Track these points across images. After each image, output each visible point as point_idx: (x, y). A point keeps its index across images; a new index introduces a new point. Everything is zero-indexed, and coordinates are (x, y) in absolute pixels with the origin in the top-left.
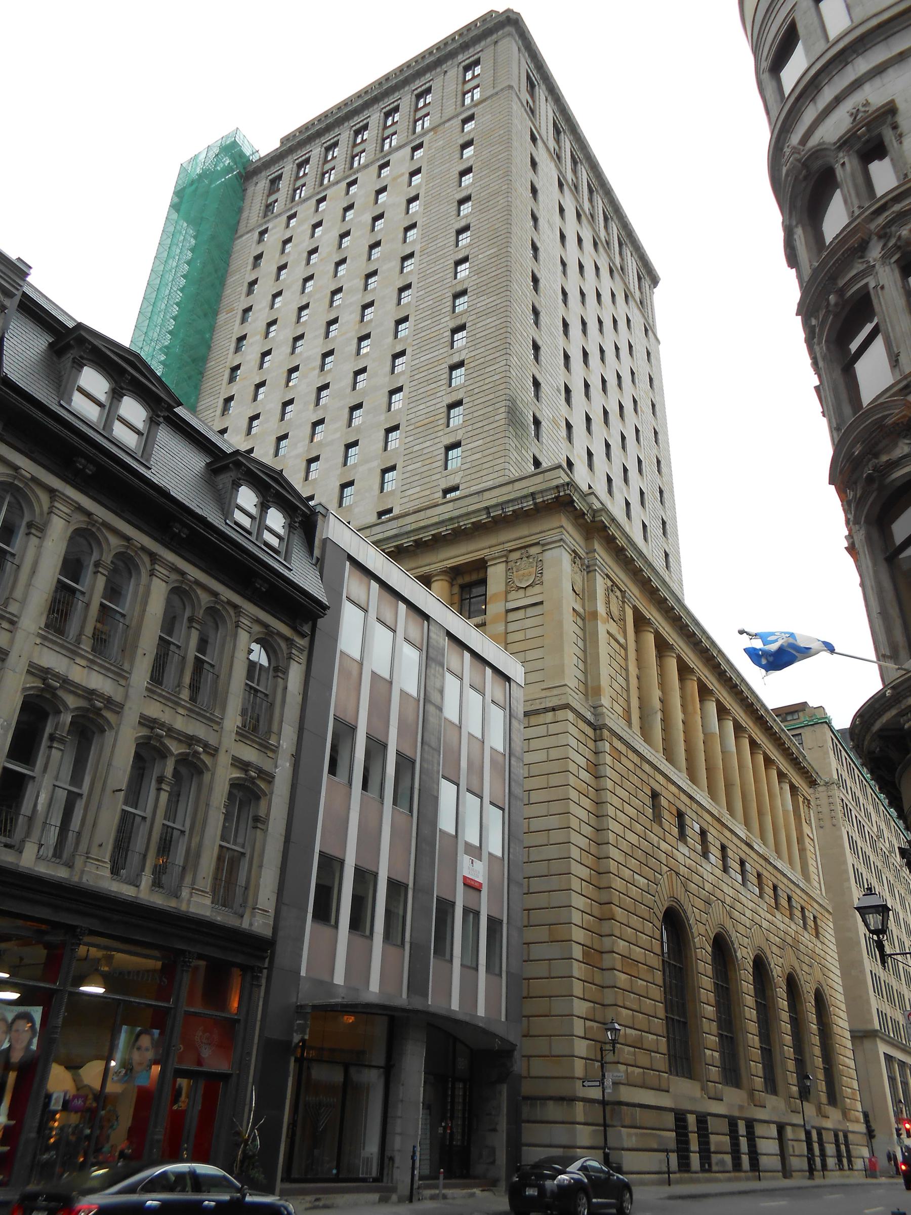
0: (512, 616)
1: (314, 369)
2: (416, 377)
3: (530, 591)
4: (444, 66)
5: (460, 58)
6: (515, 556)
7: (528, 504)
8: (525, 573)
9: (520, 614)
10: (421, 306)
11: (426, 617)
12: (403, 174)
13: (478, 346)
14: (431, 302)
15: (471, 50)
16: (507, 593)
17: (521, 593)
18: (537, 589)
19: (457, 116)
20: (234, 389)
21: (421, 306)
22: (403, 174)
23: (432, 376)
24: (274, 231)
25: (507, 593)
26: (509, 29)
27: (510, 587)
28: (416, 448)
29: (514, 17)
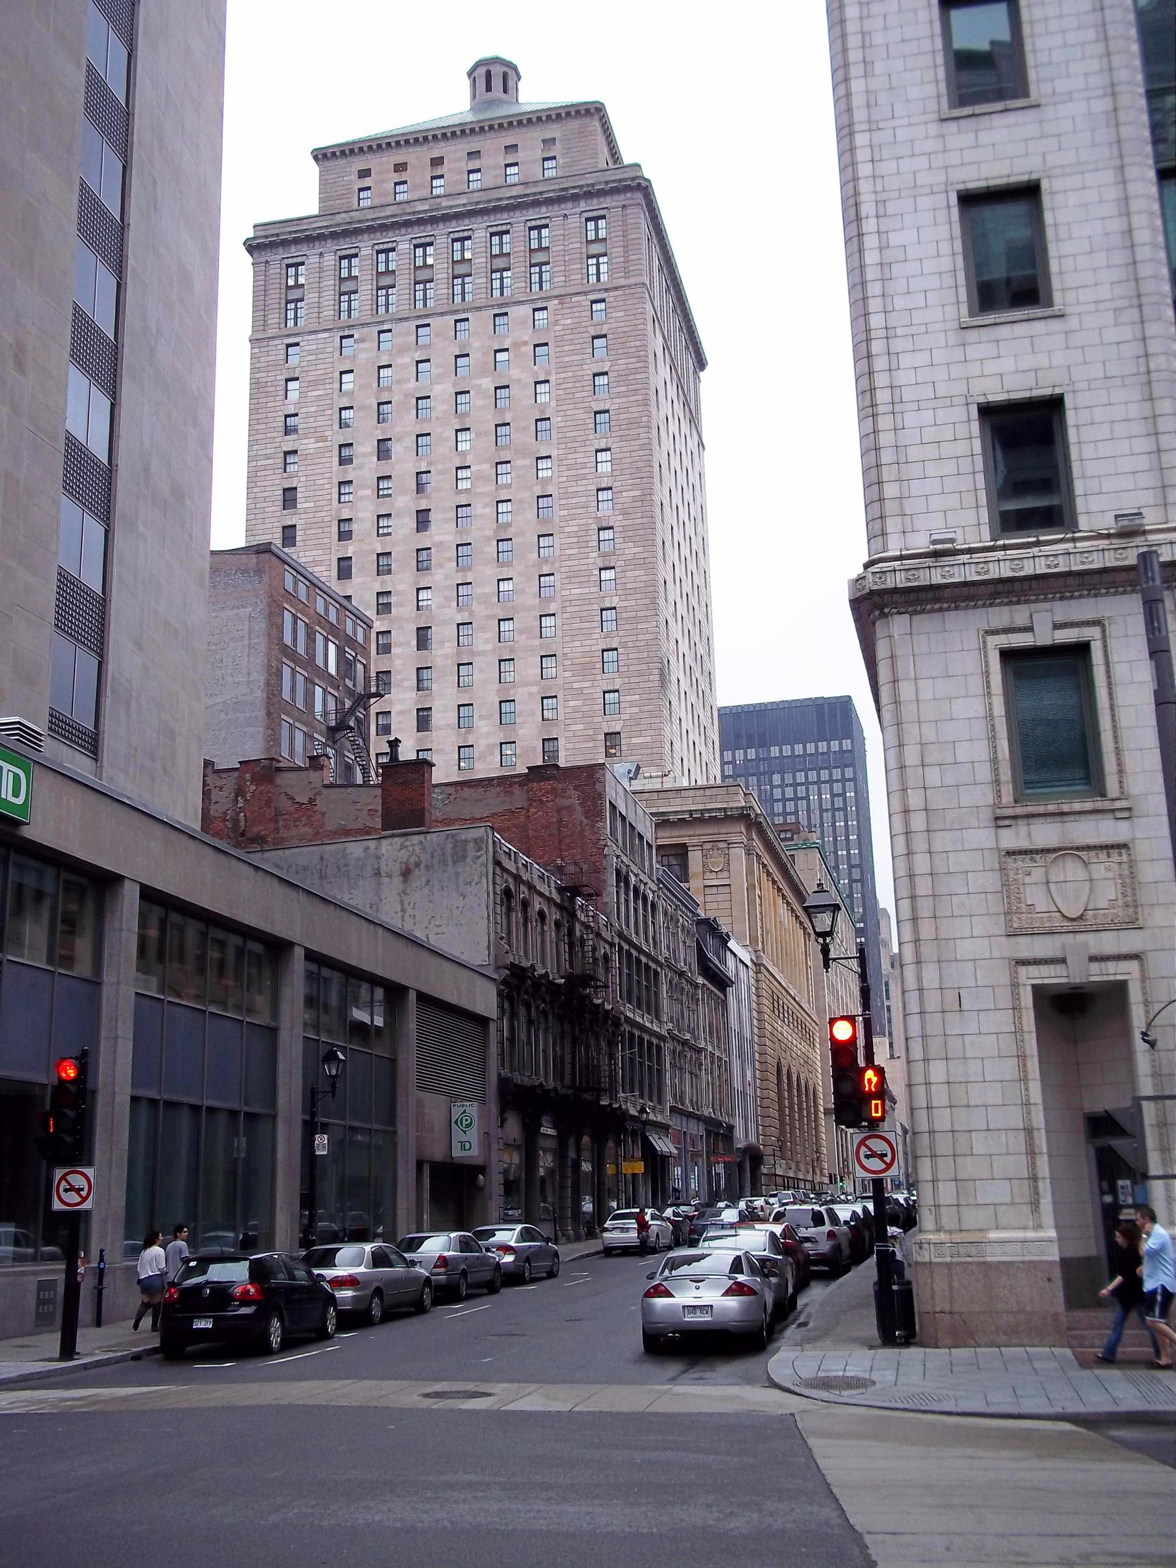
0: (708, 891)
1: (450, 559)
2: (568, 610)
3: (720, 875)
4: (563, 206)
5: (583, 205)
6: (708, 846)
7: (720, 815)
8: (717, 862)
9: (714, 890)
10: (567, 530)
11: (735, 955)
12: (526, 343)
13: (629, 597)
14: (576, 529)
16: (704, 873)
17: (713, 875)
18: (725, 874)
19: (585, 293)
20: (350, 550)
21: (567, 530)
22: (526, 343)
23: (585, 614)
25: (704, 873)
26: (639, 197)
27: (706, 869)
28: (576, 685)
29: (644, 184)
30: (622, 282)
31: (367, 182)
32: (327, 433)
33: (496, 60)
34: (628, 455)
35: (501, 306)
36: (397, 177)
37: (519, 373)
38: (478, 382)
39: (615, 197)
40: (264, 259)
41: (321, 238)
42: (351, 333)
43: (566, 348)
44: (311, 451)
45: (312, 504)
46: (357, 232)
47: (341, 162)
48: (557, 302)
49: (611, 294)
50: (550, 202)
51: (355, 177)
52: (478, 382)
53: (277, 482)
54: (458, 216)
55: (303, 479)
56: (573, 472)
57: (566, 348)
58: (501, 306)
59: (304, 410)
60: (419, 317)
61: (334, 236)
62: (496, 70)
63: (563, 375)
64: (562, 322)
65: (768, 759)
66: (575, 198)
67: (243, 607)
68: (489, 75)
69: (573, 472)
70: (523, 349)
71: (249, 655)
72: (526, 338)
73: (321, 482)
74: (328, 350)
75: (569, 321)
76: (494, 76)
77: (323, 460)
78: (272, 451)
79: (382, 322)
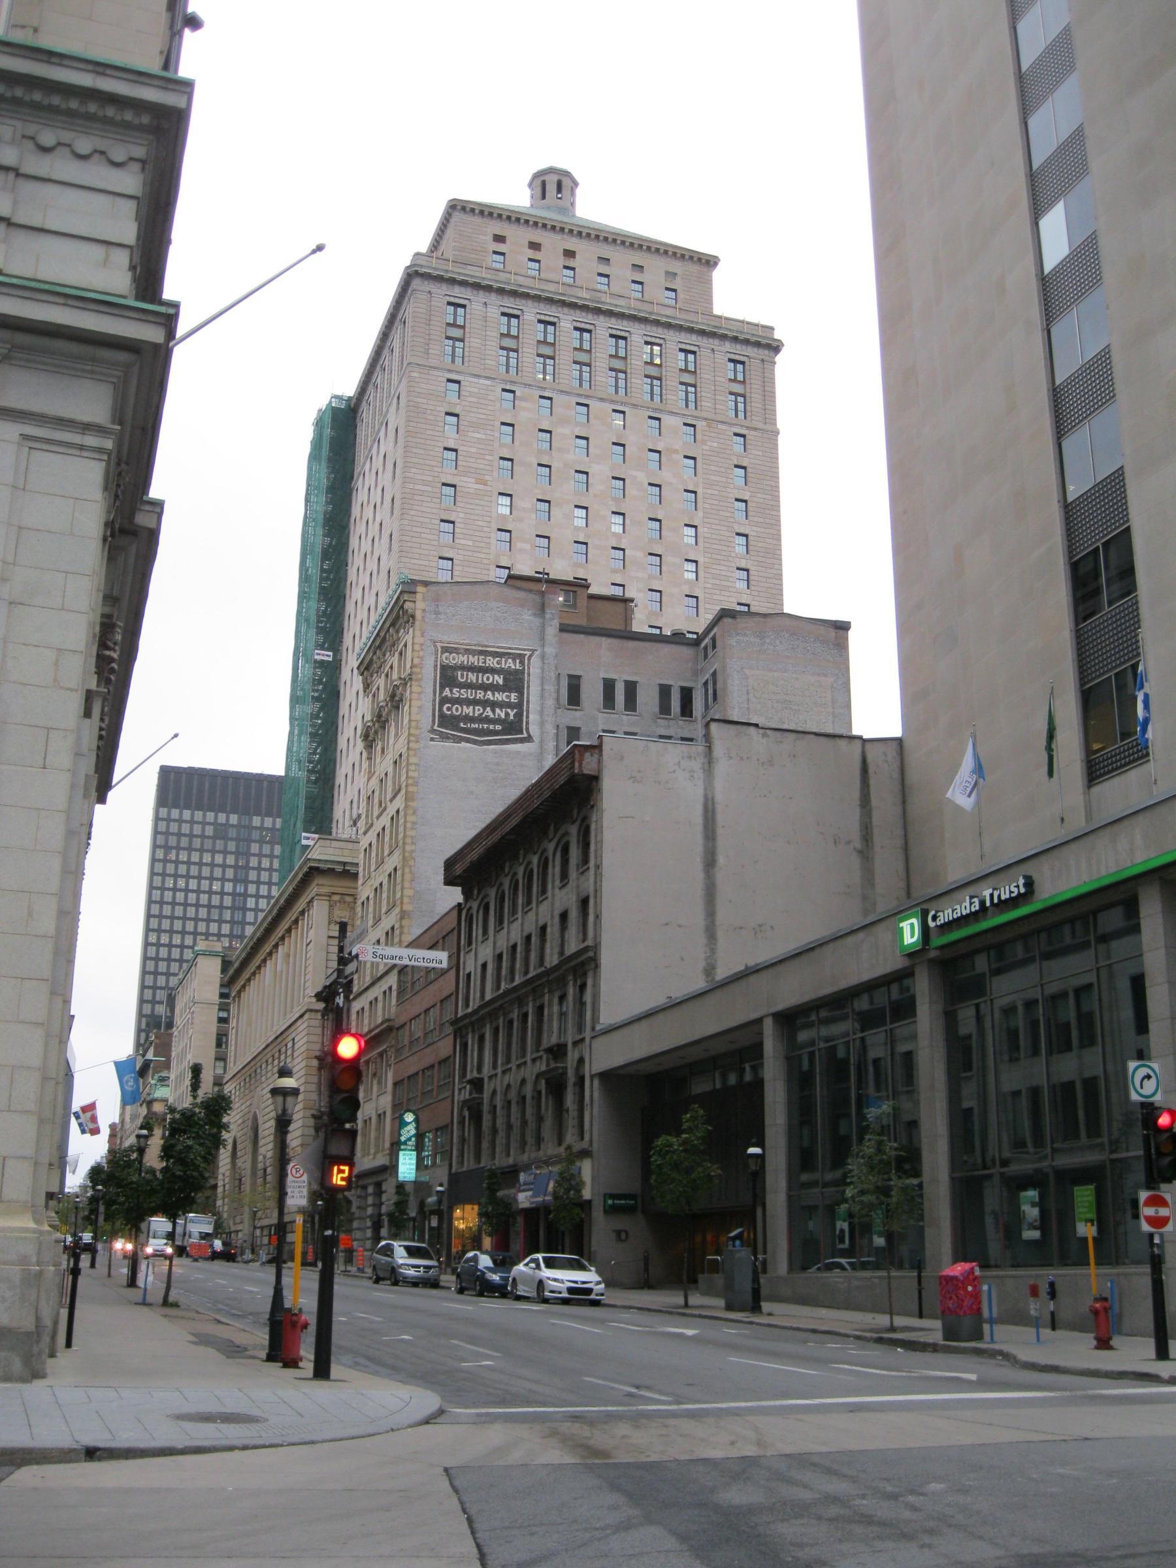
12: (676, 451)
15: (738, 346)
22: (676, 451)
24: (524, 404)
30: (761, 426)
31: (501, 247)
32: (487, 478)
33: (567, 174)
34: (763, 580)
35: (655, 410)
36: (531, 254)
37: (676, 475)
38: (634, 473)
39: (755, 350)
40: (428, 289)
41: (488, 289)
42: (513, 388)
43: (713, 468)
44: (472, 491)
45: (470, 543)
46: (526, 296)
47: (477, 220)
48: (704, 423)
49: (753, 433)
50: (702, 333)
51: (490, 238)
52: (634, 473)
53: (435, 511)
54: (621, 316)
55: (462, 515)
56: (717, 582)
57: (713, 468)
58: (655, 410)
59: (465, 448)
60: (580, 395)
61: (501, 291)
62: (552, 181)
63: (709, 491)
64: (709, 443)
65: (250, 828)
66: (724, 337)
67: (825, 675)
68: (544, 184)
69: (717, 582)
70: (675, 456)
71: (833, 722)
72: (677, 447)
73: (480, 523)
74: (490, 397)
75: (715, 445)
76: (554, 184)
77: (482, 503)
78: (430, 479)
79: (544, 389)
